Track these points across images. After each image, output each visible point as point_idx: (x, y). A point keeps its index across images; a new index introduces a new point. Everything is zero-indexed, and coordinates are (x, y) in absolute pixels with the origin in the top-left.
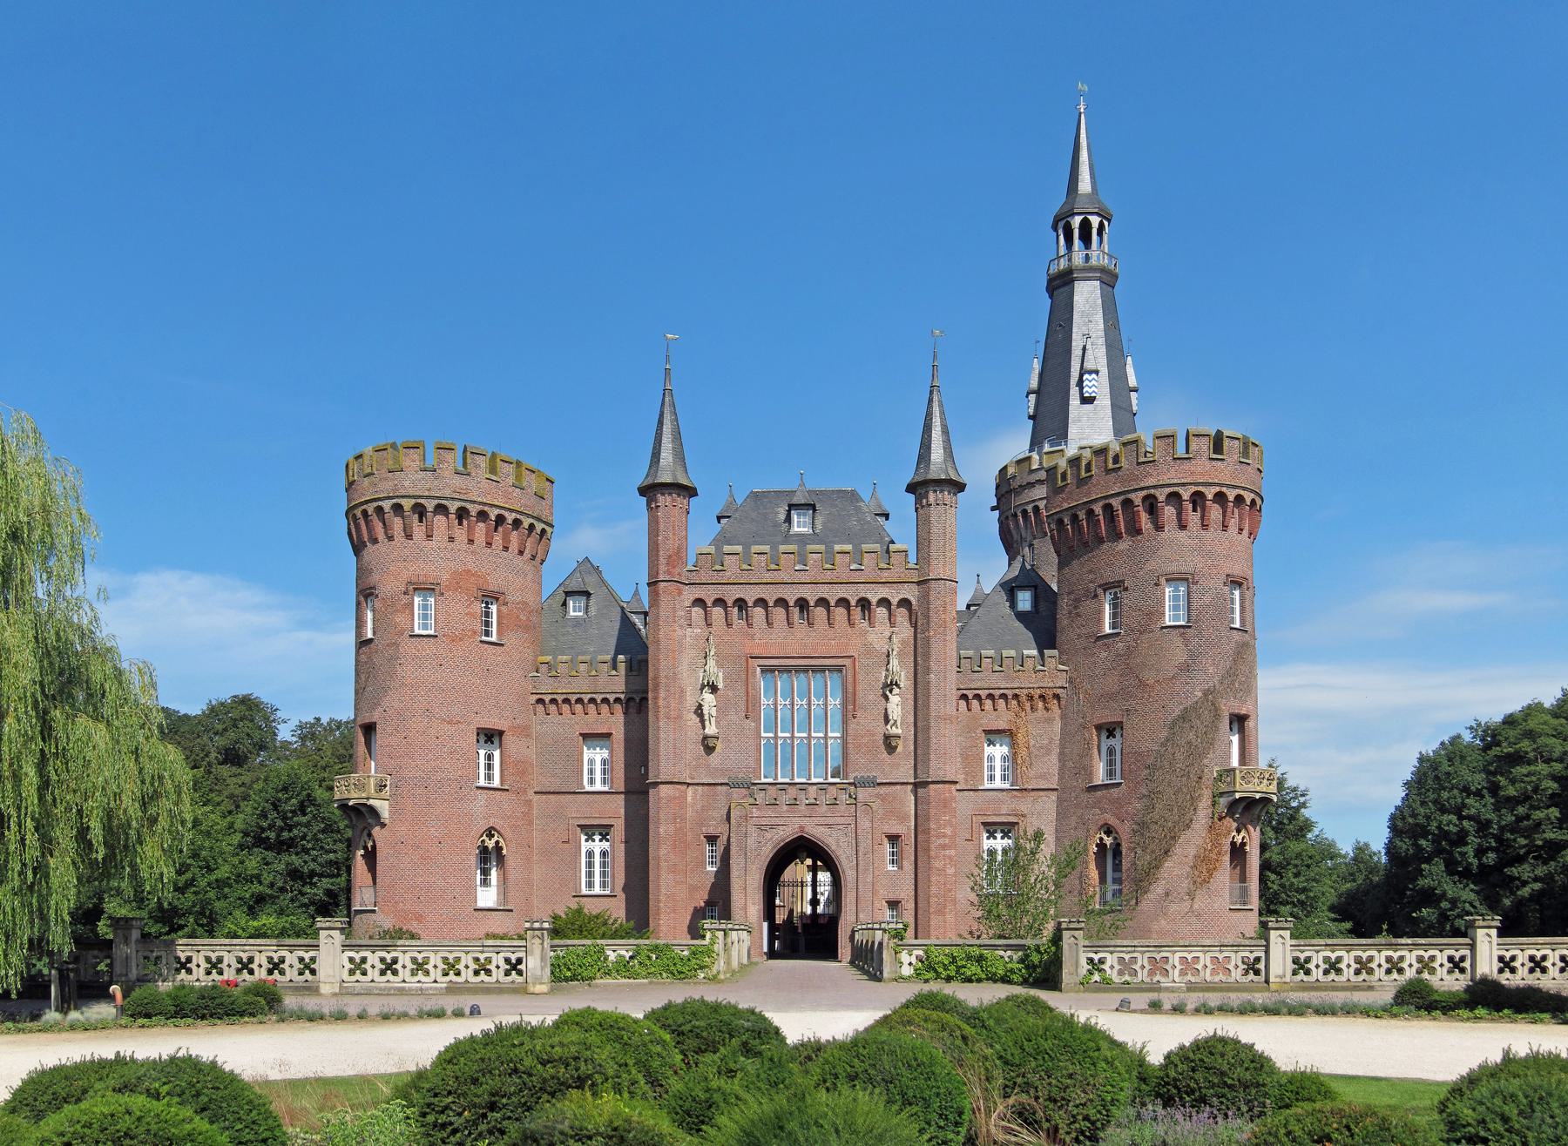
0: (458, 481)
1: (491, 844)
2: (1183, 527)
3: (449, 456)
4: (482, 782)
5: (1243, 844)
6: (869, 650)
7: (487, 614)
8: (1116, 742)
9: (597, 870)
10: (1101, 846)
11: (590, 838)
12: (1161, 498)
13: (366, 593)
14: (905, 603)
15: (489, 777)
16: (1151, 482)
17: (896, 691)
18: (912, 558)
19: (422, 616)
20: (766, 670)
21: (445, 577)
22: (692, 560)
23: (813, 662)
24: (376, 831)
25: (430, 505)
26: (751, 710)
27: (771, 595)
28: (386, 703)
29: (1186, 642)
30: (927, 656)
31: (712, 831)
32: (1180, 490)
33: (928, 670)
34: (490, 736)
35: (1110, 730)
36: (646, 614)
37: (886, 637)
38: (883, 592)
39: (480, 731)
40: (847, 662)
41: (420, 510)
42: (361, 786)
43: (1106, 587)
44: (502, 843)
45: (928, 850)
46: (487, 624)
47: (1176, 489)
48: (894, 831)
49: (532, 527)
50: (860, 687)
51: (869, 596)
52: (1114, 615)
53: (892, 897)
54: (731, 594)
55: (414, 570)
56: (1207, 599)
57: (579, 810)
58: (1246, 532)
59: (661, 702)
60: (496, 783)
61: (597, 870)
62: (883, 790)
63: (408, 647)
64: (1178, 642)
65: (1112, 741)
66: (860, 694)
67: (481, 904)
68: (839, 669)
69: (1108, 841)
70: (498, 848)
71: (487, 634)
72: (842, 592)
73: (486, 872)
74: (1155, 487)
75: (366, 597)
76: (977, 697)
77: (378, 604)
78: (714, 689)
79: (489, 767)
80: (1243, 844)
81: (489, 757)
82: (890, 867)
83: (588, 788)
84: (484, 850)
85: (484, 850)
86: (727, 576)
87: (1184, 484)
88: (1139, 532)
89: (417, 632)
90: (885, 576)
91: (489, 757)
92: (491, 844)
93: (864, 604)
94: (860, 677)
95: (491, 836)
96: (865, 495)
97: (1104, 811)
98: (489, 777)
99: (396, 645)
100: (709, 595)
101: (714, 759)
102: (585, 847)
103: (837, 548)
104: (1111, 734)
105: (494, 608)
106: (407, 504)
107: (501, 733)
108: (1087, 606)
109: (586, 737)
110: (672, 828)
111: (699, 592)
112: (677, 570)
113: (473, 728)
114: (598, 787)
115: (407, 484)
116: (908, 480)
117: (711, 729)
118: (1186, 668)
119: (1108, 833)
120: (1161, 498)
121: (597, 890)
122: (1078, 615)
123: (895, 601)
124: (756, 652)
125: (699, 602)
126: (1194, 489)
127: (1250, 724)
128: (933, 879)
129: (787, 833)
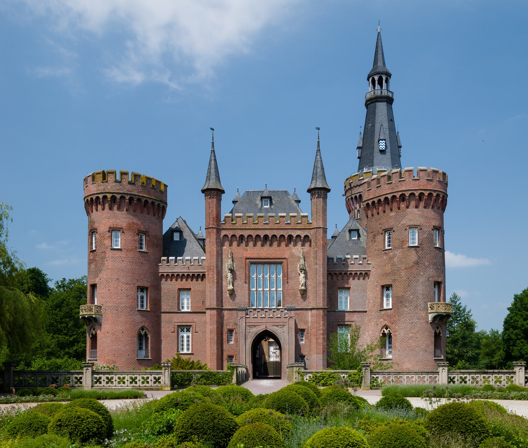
0: (129, 187)
1: (143, 333)
4: (139, 308)
6: (292, 256)
7: (141, 240)
8: (390, 292)
9: (185, 343)
10: (384, 334)
11: (182, 330)
12: (407, 195)
13: (93, 231)
14: (306, 236)
20: (252, 263)
26: (248, 280)
27: (254, 234)
28: (101, 275)
31: (231, 328)
32: (415, 192)
35: (387, 287)
36: (204, 240)
38: (298, 233)
39: (138, 287)
40: (284, 260)
42: (91, 310)
43: (386, 231)
46: (141, 244)
47: (413, 192)
49: (159, 204)
50: (289, 270)
51: (293, 234)
52: (389, 242)
54: (238, 233)
55: (111, 222)
56: (425, 236)
57: (177, 319)
61: (185, 343)
62: (298, 312)
65: (388, 292)
66: (289, 273)
68: (281, 263)
69: (386, 332)
70: (146, 335)
71: (141, 248)
72: (282, 232)
74: (405, 191)
75: (92, 233)
76: (336, 274)
77: (97, 236)
79: (142, 302)
80: (440, 333)
81: (142, 298)
86: (238, 226)
87: (416, 190)
90: (299, 226)
92: (143, 333)
93: (290, 237)
94: (289, 266)
95: (143, 329)
96: (291, 192)
97: (385, 320)
102: (181, 334)
103: (280, 214)
104: (388, 289)
105: (144, 237)
106: (109, 196)
107: (147, 288)
108: (380, 238)
109: (180, 290)
113: (136, 286)
114: (185, 310)
115: (109, 187)
119: (387, 328)
121: (185, 351)
122: (375, 241)
123: (303, 236)
126: (420, 192)
129: (261, 329)
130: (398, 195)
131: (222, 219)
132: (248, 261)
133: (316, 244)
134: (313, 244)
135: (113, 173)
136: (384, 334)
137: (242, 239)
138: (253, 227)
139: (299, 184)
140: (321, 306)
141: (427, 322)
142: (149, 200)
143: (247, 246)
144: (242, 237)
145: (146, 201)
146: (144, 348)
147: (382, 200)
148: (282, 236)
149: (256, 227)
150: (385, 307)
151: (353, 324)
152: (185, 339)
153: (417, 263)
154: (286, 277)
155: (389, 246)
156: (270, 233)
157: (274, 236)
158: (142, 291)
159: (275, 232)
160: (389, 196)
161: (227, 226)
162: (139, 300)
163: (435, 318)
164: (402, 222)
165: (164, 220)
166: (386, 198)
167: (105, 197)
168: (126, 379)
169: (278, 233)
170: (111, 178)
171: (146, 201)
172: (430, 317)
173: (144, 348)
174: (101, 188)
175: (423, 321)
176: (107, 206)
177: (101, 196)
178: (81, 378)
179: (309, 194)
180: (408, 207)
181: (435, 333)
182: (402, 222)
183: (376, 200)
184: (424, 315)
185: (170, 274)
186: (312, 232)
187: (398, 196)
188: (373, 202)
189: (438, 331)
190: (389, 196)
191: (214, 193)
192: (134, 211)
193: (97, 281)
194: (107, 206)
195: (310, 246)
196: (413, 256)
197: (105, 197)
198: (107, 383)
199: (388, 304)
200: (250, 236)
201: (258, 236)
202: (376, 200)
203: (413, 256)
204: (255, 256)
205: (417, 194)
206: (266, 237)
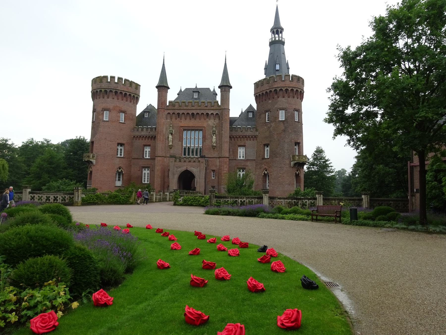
0: (115, 85)
2: (284, 97)
3: (113, 79)
4: (119, 156)
5: (299, 174)
10: (264, 174)
12: (278, 90)
14: (217, 114)
15: (121, 155)
16: (276, 86)
17: (215, 135)
18: (219, 103)
19: (106, 116)
20: (184, 130)
21: (111, 107)
22: (168, 104)
23: (196, 128)
24: (92, 167)
25: (108, 91)
26: (181, 139)
27: (185, 112)
28: (96, 136)
30: (222, 127)
33: (222, 130)
35: (267, 145)
37: (211, 122)
38: (212, 112)
40: (203, 128)
41: (106, 91)
42: (89, 157)
43: (266, 111)
44: (123, 170)
45: (221, 174)
48: (213, 169)
50: (206, 134)
52: (268, 118)
53: (213, 185)
55: (104, 106)
56: (289, 114)
58: (299, 99)
59: (159, 137)
60: (122, 156)
63: (102, 124)
64: (282, 124)
67: (116, 185)
68: (201, 130)
69: (266, 173)
70: (122, 172)
78: (172, 134)
79: (121, 152)
80: (299, 174)
82: (213, 178)
83: (145, 158)
86: (176, 107)
88: (273, 98)
89: (104, 120)
90: (212, 108)
91: (121, 150)
92: (120, 171)
93: (207, 114)
95: (120, 169)
97: (265, 165)
98: (121, 155)
99: (99, 123)
100: (171, 112)
106: (103, 90)
110: (160, 167)
112: (163, 106)
113: (116, 143)
116: (219, 85)
117: (171, 143)
118: (284, 131)
119: (266, 171)
120: (278, 90)
123: (215, 114)
124: (182, 125)
127: (301, 145)
128: (222, 181)
130: (273, 90)
131: (168, 104)
132: (182, 128)
135: (106, 77)
136: (264, 174)
138: (185, 108)
139: (213, 83)
141: (290, 167)
143: (181, 119)
144: (178, 114)
145: (126, 94)
146: (121, 180)
150: (266, 157)
151: (247, 167)
152: (146, 175)
154: (204, 138)
155: (268, 120)
156: (195, 112)
157: (198, 114)
160: (268, 91)
161: (170, 108)
162: (119, 151)
163: (295, 164)
164: (276, 106)
165: (137, 105)
167: (101, 91)
169: (200, 112)
170: (104, 81)
171: (126, 94)
173: (121, 180)
174: (99, 86)
176: (101, 95)
177: (98, 90)
178: (73, 197)
180: (278, 97)
181: (296, 174)
182: (276, 106)
183: (261, 93)
184: (288, 162)
185: (139, 136)
186: (220, 111)
187: (273, 91)
188: (260, 95)
189: (297, 173)
190: (268, 91)
191: (163, 87)
192: (118, 99)
193: (94, 139)
194: (101, 95)
197: (101, 91)
200: (183, 113)
201: (188, 114)
202: (261, 93)
204: (186, 125)
205: (284, 90)
206: (193, 114)
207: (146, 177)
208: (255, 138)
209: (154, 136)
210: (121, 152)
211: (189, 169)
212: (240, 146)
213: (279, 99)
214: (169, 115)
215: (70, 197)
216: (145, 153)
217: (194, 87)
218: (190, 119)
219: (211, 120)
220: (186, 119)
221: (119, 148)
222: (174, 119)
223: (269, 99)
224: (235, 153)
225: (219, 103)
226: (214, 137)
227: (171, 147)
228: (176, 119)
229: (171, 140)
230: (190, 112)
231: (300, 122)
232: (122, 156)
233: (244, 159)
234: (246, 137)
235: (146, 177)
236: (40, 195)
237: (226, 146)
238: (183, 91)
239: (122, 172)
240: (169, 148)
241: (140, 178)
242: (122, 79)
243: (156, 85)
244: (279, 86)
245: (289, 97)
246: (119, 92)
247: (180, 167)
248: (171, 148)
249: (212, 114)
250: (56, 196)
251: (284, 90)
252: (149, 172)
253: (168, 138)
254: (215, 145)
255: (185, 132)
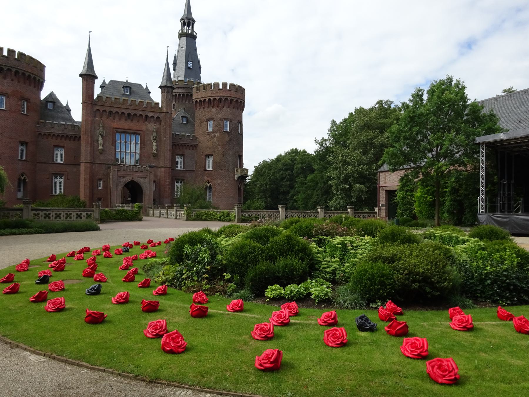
2: (229, 107)
4: (20, 158)
14: (158, 118)
15: (22, 157)
16: (221, 95)
18: (160, 106)
26: (114, 143)
27: (120, 111)
29: (229, 136)
31: (100, 177)
34: (22, 143)
38: (152, 114)
40: (142, 132)
43: (208, 120)
44: (26, 178)
56: (234, 126)
60: (24, 158)
64: (227, 136)
68: (139, 134)
69: (208, 185)
70: (25, 179)
72: (141, 113)
73: (19, 187)
78: (102, 136)
79: (22, 153)
81: (22, 150)
84: (20, 179)
85: (20, 179)
91: (22, 150)
92: (23, 178)
93: (147, 116)
95: (22, 175)
97: (208, 177)
98: (22, 157)
100: (102, 109)
101: (102, 157)
107: (27, 143)
111: (98, 108)
117: (101, 147)
119: (209, 183)
123: (156, 117)
124: (115, 127)
125: (98, 110)
130: (218, 98)
132: (115, 130)
133: (165, 123)
134: (163, 123)
137: (110, 114)
138: (119, 106)
140: (168, 165)
141: (234, 179)
142: (31, 75)
143: (114, 119)
144: (111, 112)
147: (207, 100)
148: (141, 115)
149: (122, 106)
153: (229, 142)
156: (132, 112)
157: (135, 114)
158: (22, 145)
159: (136, 112)
160: (212, 98)
163: (239, 178)
164: (220, 116)
166: (210, 100)
168: (62, 215)
172: (236, 177)
175: (232, 179)
179: (160, 90)
180: (223, 107)
190: (212, 98)
195: (160, 124)
196: (227, 138)
198: (45, 218)
199: (209, 167)
200: (117, 112)
201: (123, 113)
203: (227, 138)
204: (121, 127)
207: (58, 187)
208: (195, 148)
209: (78, 137)
210: (22, 154)
211: (136, 179)
212: (178, 155)
213: (224, 109)
214: (98, 113)
215: (87, 214)
216: (55, 156)
217: (125, 81)
218: (126, 120)
219: (151, 124)
220: (120, 119)
221: (20, 148)
222: (104, 118)
223: (213, 107)
224: (173, 162)
225: (160, 106)
226: (155, 144)
227: (102, 152)
228: (107, 118)
229: (102, 143)
230: (126, 112)
231: (241, 134)
232: (62, 162)
233: (182, 169)
234: (185, 145)
235: (58, 187)
236: (47, 213)
237: (168, 155)
238: (107, 82)
239: (25, 179)
240: (98, 153)
241: (49, 188)
242: (14, 52)
243: (80, 72)
244: (224, 95)
245: (234, 108)
246: (21, 72)
247: (124, 177)
248: (101, 153)
249: (152, 117)
250: (89, 213)
251: (229, 100)
252: (62, 180)
253: (98, 140)
254: (155, 152)
255: (118, 135)
